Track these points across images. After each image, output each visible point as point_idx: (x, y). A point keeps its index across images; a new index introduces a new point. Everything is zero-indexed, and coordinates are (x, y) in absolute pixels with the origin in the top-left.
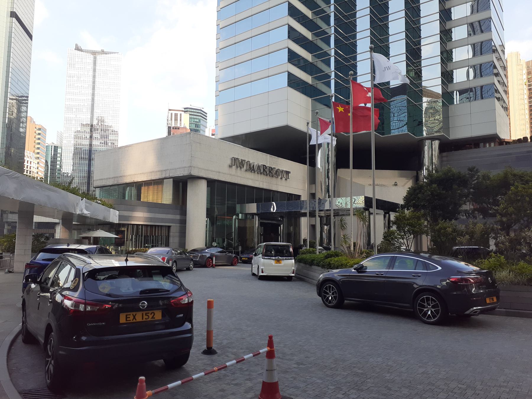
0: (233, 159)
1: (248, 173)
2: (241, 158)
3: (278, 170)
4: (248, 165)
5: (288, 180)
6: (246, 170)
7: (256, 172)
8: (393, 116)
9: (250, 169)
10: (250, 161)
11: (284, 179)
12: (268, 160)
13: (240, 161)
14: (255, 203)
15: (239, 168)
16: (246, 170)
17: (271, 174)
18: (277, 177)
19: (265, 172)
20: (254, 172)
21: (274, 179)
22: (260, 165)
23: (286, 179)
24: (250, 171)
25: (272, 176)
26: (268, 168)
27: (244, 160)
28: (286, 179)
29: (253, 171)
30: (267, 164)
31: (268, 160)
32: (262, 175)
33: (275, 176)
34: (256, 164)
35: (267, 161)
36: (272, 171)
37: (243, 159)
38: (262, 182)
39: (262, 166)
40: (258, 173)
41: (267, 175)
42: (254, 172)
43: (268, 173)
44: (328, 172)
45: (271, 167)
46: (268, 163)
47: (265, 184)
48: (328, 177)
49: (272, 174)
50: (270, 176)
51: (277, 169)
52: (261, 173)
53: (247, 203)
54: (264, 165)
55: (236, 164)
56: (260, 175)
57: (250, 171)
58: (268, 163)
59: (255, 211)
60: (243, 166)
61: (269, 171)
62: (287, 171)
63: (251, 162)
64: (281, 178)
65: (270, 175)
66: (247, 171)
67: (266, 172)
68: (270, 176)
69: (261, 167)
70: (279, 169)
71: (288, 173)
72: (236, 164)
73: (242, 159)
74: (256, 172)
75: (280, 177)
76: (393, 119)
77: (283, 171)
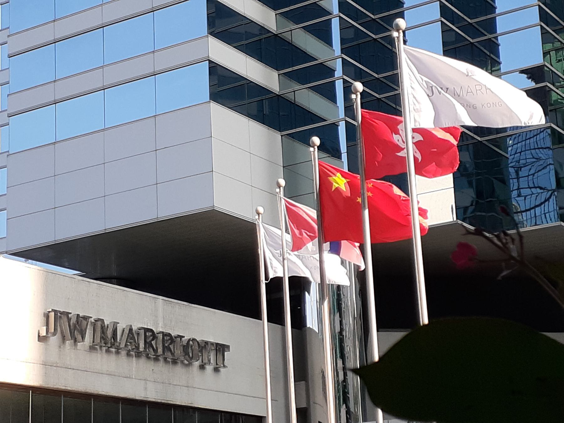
0: (52, 315)
1: (99, 355)
2: (75, 310)
3: (191, 342)
4: (98, 334)
5: (222, 370)
6: (92, 348)
8: (513, 175)
9: (105, 344)
10: (103, 320)
11: (209, 368)
12: (160, 314)
13: (73, 320)
16: (92, 348)
17: (169, 354)
18: (190, 364)
19: (151, 350)
20: (118, 353)
21: (179, 369)
22: (134, 328)
23: (216, 370)
24: (104, 349)
25: (175, 362)
26: (160, 336)
27: (86, 318)
28: (216, 370)
30: (157, 324)
31: (160, 314)
32: (143, 360)
33: (182, 362)
34: (124, 327)
35: (157, 317)
36: (172, 347)
37: (81, 315)
38: (143, 382)
39: (142, 332)
40: (128, 355)
41: (156, 359)
42: (118, 353)
43: (160, 351)
44: (341, 341)
45: (169, 335)
47: (150, 385)
48: (343, 357)
49: (173, 354)
50: (169, 362)
51: (189, 340)
52: (138, 355)
54: (147, 330)
55: (62, 332)
56: (134, 358)
57: (104, 349)
60: (83, 338)
61: (163, 345)
62: (217, 344)
63: (106, 323)
64: (202, 367)
65: (165, 359)
66: (96, 349)
67: (155, 351)
68: (169, 362)
69: (138, 334)
70: (194, 340)
71: (221, 349)
72: (59, 329)
73: (78, 315)
74: (124, 353)
75: (197, 364)
76: (516, 184)
77: (207, 343)
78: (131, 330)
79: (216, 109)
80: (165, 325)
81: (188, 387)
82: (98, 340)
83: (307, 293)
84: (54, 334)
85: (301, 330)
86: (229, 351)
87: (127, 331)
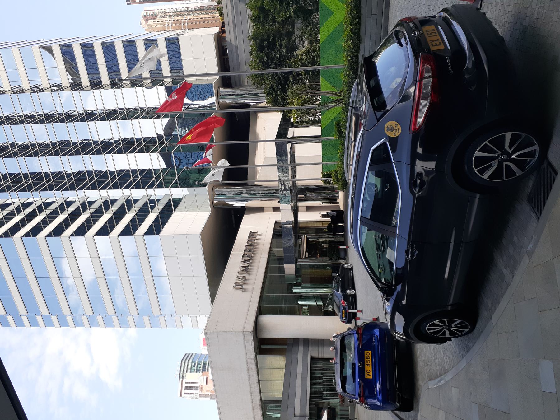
7: (251, 264)
14: (284, 265)
15: (246, 282)
29: (249, 268)
34: (241, 264)
46: (241, 253)
47: (262, 256)
53: (284, 273)
54: (243, 257)
58: (241, 253)
59: (292, 266)
60: (245, 277)
78: (242, 262)
79: (161, 233)
80: (242, 251)
81: (264, 244)
82: (245, 272)
83: (233, 206)
84: (242, 286)
85: (246, 208)
86: (252, 231)
87: (243, 263)
